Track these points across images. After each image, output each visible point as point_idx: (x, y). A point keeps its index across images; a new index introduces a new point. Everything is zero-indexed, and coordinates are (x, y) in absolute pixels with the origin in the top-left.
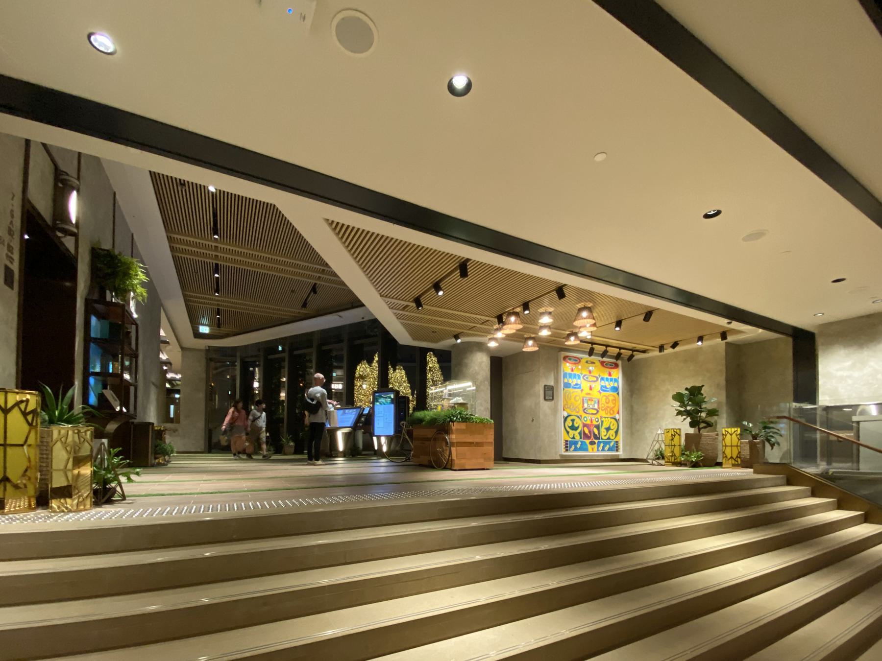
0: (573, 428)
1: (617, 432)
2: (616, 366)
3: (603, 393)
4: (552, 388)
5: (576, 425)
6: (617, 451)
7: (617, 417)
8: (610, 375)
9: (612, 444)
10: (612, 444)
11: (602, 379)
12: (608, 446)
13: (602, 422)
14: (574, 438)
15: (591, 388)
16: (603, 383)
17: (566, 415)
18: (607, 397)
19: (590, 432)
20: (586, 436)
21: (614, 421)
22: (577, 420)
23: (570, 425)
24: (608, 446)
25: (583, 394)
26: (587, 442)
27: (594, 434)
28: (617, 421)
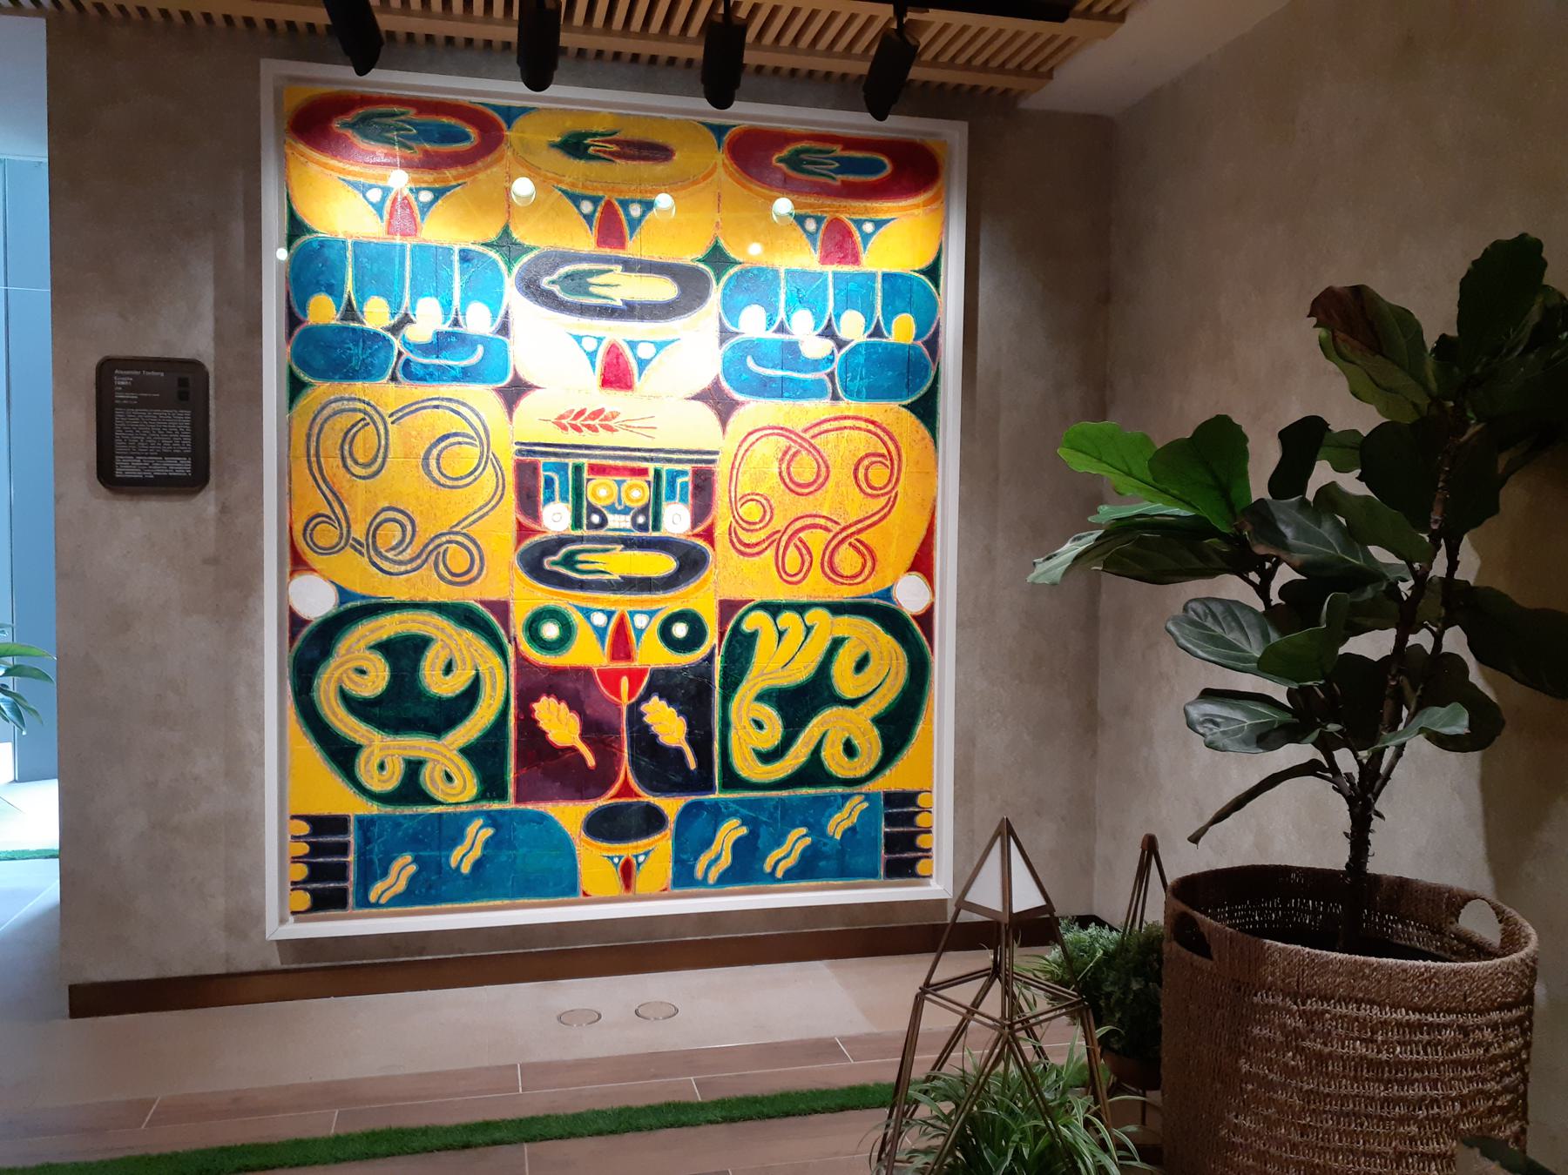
0: (405, 707)
1: (898, 725)
2: (911, 172)
3: (755, 412)
4: (184, 384)
5: (439, 684)
6: (903, 866)
7: (910, 596)
8: (840, 244)
9: (838, 824)
10: (838, 824)
11: (756, 284)
12: (797, 841)
13: (740, 648)
14: (411, 789)
15: (616, 375)
16: (753, 323)
17: (315, 599)
18: (798, 442)
19: (595, 730)
20: (552, 769)
21: (864, 633)
22: (449, 640)
23: (376, 679)
24: (797, 841)
25: (535, 422)
26: (570, 815)
27: (645, 740)
28: (911, 634)
